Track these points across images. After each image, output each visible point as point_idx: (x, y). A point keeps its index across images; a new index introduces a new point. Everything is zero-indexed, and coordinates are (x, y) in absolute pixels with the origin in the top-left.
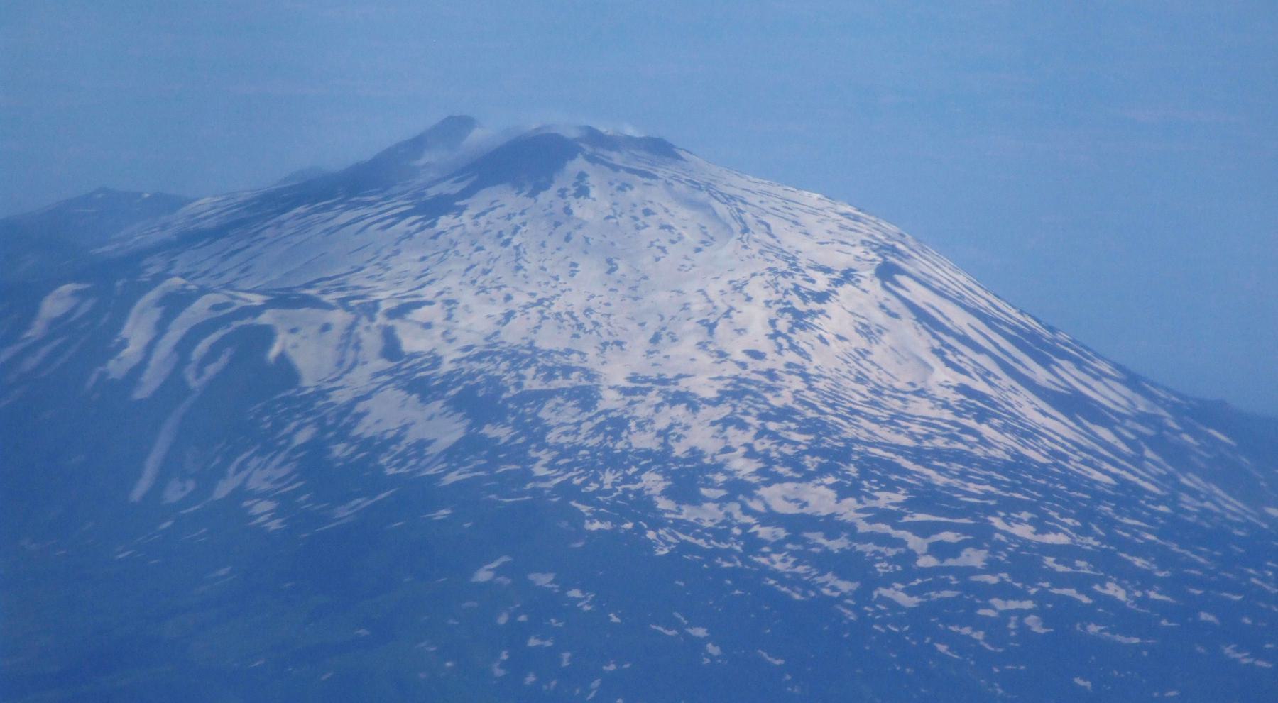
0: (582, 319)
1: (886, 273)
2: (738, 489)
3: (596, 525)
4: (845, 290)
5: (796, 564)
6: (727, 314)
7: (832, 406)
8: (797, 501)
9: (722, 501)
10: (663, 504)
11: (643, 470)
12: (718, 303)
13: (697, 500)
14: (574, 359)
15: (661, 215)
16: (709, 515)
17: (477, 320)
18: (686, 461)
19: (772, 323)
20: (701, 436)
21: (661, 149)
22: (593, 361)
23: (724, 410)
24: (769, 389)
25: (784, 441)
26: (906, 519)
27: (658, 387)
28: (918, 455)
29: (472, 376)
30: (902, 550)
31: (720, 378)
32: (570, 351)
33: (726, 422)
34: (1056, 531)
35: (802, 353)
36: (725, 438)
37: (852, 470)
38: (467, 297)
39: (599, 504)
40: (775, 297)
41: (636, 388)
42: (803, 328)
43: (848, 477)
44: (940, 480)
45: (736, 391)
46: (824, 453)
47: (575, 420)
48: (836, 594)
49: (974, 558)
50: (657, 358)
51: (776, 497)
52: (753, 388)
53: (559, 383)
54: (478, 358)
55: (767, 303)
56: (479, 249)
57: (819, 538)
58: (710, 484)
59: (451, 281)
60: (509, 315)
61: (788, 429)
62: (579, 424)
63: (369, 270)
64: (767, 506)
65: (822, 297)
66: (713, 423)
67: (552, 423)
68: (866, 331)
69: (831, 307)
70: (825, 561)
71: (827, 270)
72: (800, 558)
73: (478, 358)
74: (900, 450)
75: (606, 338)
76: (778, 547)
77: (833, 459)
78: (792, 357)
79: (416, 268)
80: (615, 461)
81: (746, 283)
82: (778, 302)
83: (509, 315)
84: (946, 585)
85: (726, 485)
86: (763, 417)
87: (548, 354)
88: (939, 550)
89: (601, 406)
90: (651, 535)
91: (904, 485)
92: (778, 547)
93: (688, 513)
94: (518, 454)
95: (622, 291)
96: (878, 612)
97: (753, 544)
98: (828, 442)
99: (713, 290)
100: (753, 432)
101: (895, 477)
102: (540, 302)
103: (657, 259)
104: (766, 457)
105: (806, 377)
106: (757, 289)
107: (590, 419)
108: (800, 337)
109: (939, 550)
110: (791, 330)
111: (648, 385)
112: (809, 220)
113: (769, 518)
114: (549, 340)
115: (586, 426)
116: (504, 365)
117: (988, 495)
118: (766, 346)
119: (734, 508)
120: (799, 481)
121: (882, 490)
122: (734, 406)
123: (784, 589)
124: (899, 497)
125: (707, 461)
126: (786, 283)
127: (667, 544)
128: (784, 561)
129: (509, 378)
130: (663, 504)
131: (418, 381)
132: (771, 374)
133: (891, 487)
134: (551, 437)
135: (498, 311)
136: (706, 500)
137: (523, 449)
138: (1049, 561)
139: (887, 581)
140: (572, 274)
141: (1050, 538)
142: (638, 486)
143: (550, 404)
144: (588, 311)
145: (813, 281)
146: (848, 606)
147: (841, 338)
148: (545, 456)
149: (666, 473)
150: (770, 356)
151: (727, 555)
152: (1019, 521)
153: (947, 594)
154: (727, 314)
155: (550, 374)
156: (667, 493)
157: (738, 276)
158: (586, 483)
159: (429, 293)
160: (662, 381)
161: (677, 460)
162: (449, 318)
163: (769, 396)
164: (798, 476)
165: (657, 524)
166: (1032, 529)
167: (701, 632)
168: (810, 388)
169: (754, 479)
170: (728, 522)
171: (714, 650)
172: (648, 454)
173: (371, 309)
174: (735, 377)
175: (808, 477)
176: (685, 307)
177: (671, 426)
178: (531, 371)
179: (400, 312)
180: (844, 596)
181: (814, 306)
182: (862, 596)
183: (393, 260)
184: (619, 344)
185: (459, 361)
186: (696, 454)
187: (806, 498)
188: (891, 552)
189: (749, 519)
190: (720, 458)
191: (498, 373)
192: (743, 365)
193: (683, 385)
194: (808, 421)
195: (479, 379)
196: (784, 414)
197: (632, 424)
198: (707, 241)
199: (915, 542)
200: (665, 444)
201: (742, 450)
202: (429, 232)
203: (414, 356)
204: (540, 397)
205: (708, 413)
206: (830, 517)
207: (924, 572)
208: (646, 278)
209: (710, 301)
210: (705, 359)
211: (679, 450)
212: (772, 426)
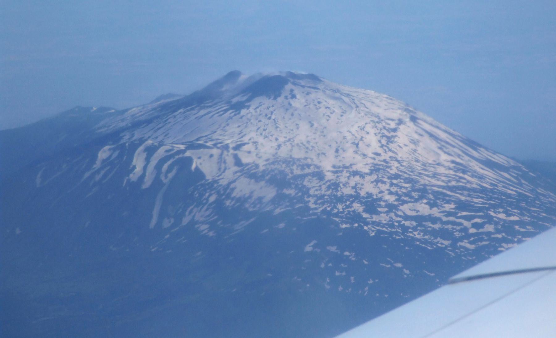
0: (307, 145)
1: (414, 119)
2: (391, 208)
3: (344, 226)
4: (402, 127)
5: (424, 235)
6: (362, 139)
7: (412, 172)
8: (415, 210)
9: (386, 212)
10: (365, 215)
11: (352, 202)
12: (356, 135)
13: (378, 213)
14: (309, 161)
15: (324, 103)
16: (383, 218)
17: (267, 148)
18: (367, 198)
19: (380, 141)
20: (368, 187)
21: (313, 78)
22: (316, 162)
23: (374, 177)
24: (387, 167)
25: (401, 187)
26: (459, 215)
27: (345, 170)
28: (452, 189)
29: (273, 171)
30: (462, 227)
31: (367, 164)
32: (306, 158)
33: (377, 181)
34: (514, 215)
35: (394, 152)
36: (379, 188)
37: (431, 196)
38: (261, 140)
39: (342, 217)
40: (377, 132)
41: (337, 170)
42: (392, 142)
43: (431, 199)
44: (463, 198)
45: (375, 169)
46: (418, 190)
47: (319, 185)
48: (443, 246)
49: (490, 228)
51: (407, 209)
52: (381, 167)
53: (307, 171)
55: (375, 134)
56: (260, 121)
57: (429, 224)
58: (380, 206)
59: (251, 135)
60: (279, 146)
61: (401, 182)
62: (320, 186)
63: (219, 132)
64: (404, 213)
65: (395, 130)
66: (372, 182)
67: (310, 186)
68: (414, 142)
69: (398, 133)
70: (435, 233)
71: (392, 120)
72: (425, 232)
73: (273, 163)
74: (443, 187)
75: (318, 152)
76: (415, 229)
77: (423, 192)
78: (391, 154)
79: (237, 130)
80: (340, 200)
81: (365, 127)
82: (379, 133)
83: (279, 146)
84: (482, 240)
85: (386, 206)
86: (389, 178)
87: (299, 160)
88: (475, 225)
89: (327, 179)
90: (366, 228)
91: (453, 201)
92: (415, 229)
93: (375, 218)
95: (318, 133)
96: (461, 252)
97: (405, 229)
98: (417, 186)
99: (354, 130)
100: (388, 185)
101: (447, 198)
102: (289, 140)
103: (328, 120)
104: (396, 194)
106: (368, 128)
107: (324, 184)
108: (391, 146)
109: (475, 225)
110: (387, 144)
111: (341, 169)
112: (377, 101)
113: (407, 218)
114: (298, 154)
115: (324, 187)
116: (284, 166)
117: (483, 203)
118: (380, 150)
119: (392, 215)
120: (413, 202)
121: (445, 204)
122: (378, 175)
123: (424, 245)
124: (452, 206)
125: (375, 197)
126: (380, 126)
127: (373, 231)
128: (419, 234)
129: (287, 170)
130: (365, 215)
131: (253, 174)
132: (385, 161)
133: (448, 202)
134: (311, 192)
135: (275, 144)
136: (381, 213)
138: (517, 227)
139: (461, 239)
140: (298, 128)
141: (512, 218)
142: (353, 209)
143: (307, 179)
144: (308, 142)
145: (389, 124)
146: (449, 250)
147: (406, 145)
148: (312, 200)
149: (361, 203)
150: (383, 154)
151: (396, 233)
152: (499, 212)
153: (484, 243)
154: (362, 139)
155: (303, 167)
156: (365, 211)
157: (361, 124)
158: (332, 209)
159: (246, 139)
160: (345, 167)
161: (363, 197)
162: (256, 148)
163: (388, 170)
164: (413, 200)
165: (367, 224)
166: (504, 215)
167: (399, 265)
168: (401, 166)
169: (396, 203)
170: (391, 220)
171: (407, 272)
172: (351, 196)
173: (226, 147)
174: (372, 163)
175: (416, 201)
176: (344, 138)
177: (356, 185)
178: (295, 167)
179: (238, 147)
180: (446, 247)
181: (393, 134)
182: (454, 245)
183: (227, 128)
184: (324, 154)
185: (266, 165)
186: (369, 195)
187: (418, 209)
188: (458, 228)
189: (399, 219)
190: (379, 196)
191: (283, 169)
192: (374, 159)
193: (354, 168)
194: (406, 178)
195: (276, 171)
196: (397, 176)
197: (341, 185)
198: (344, 112)
199: (466, 223)
200: (356, 192)
201: (387, 192)
202: (238, 116)
203: (247, 164)
205: (368, 178)
206: (430, 215)
207: (473, 235)
208: (325, 128)
209: (353, 135)
210: (359, 158)
211: (363, 193)
212: (395, 181)
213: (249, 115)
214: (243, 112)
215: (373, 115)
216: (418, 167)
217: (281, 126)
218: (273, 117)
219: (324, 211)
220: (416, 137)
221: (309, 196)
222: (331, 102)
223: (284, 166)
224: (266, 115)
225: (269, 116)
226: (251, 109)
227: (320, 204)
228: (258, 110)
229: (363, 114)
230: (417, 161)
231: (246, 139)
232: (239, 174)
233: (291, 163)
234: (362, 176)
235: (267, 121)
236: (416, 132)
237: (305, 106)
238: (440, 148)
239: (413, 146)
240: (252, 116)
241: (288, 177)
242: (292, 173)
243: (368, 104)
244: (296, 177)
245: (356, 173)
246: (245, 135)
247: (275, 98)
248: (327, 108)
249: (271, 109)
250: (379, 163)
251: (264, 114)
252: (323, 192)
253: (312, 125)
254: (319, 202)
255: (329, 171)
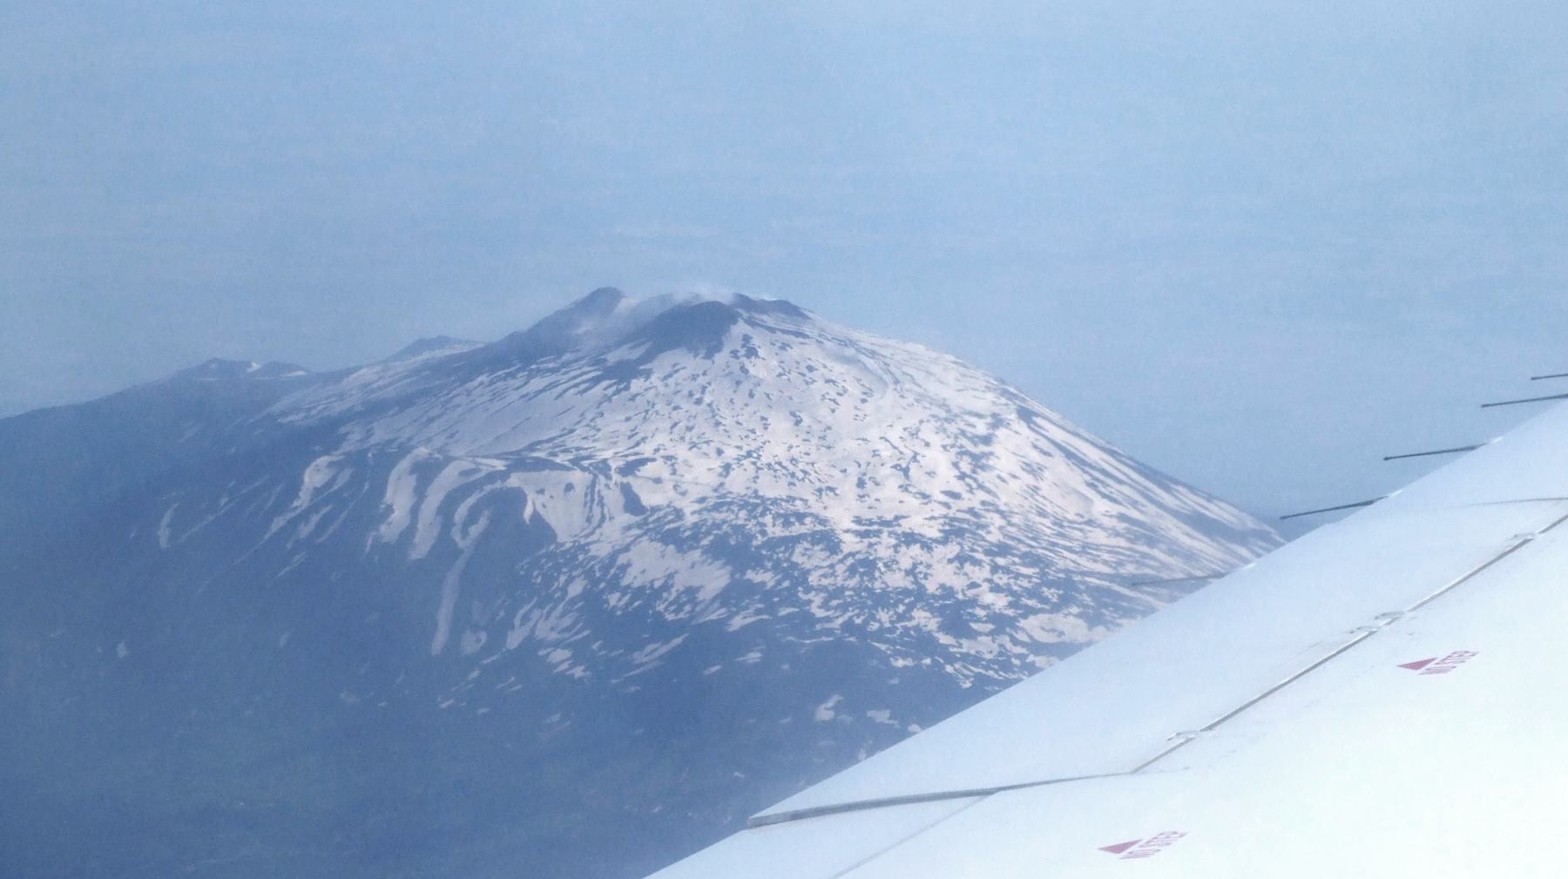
1: (1026, 415)
4: (1001, 433)
6: (914, 458)
7: (1033, 539)
11: (911, 607)
17: (701, 473)
18: (942, 597)
19: (956, 465)
20: (942, 574)
22: (816, 508)
23: (953, 549)
31: (932, 518)
32: (791, 499)
33: (961, 559)
35: (989, 492)
38: (682, 452)
41: (868, 529)
42: (983, 468)
45: (953, 531)
50: (870, 501)
53: (797, 529)
54: (717, 507)
56: (676, 408)
60: (727, 468)
62: (832, 566)
63: (580, 431)
65: (987, 440)
66: (950, 561)
67: (808, 566)
68: (1033, 470)
69: (995, 448)
73: (717, 507)
79: (625, 428)
80: (884, 599)
81: (918, 430)
82: (953, 446)
83: (727, 468)
86: (987, 552)
87: (775, 501)
89: (846, 549)
93: (967, 646)
94: (790, 598)
99: (895, 435)
102: (749, 454)
105: (1002, 514)
106: (927, 432)
107: (841, 561)
108: (982, 476)
111: (876, 527)
114: (771, 488)
115: (840, 569)
116: (743, 514)
118: (958, 487)
126: (953, 428)
129: (751, 526)
131: (674, 537)
134: (813, 579)
135: (716, 464)
137: (792, 591)
142: (914, 623)
143: (799, 549)
148: (817, 599)
150: (966, 495)
154: (914, 458)
157: (911, 422)
158: (866, 622)
161: (933, 596)
162: (674, 472)
168: (1009, 523)
172: (906, 592)
176: (875, 453)
177: (915, 566)
178: (768, 519)
179: (630, 468)
184: (831, 489)
185: (699, 512)
186: (948, 591)
190: (971, 593)
191: (740, 522)
193: (906, 526)
196: (1003, 550)
198: (868, 393)
203: (654, 510)
204: (791, 542)
205: (940, 550)
210: (913, 502)
212: (1001, 561)
213: (650, 395)
214: (637, 385)
215: (933, 402)
216: (1045, 526)
217: (728, 422)
218: (707, 399)
219: (848, 626)
220: (1035, 457)
221: (808, 590)
222: (838, 369)
223: (743, 514)
224: (691, 394)
225: (697, 396)
226: (654, 379)
227: (836, 608)
228: (671, 381)
229: (911, 399)
230: (1042, 513)
231: (647, 450)
232: (637, 532)
233: (760, 509)
234: (927, 545)
235: (694, 409)
236: (1035, 447)
237: (780, 375)
238: (1090, 485)
239: (1029, 479)
240: (657, 395)
241: (755, 543)
242: (763, 533)
243: (919, 376)
244: (773, 544)
245: (910, 538)
246: (644, 439)
247: (709, 356)
248: (828, 381)
249: (701, 380)
250: (960, 515)
251: (685, 392)
252: (839, 582)
253: (798, 423)
254: (834, 603)
255: (847, 531)
